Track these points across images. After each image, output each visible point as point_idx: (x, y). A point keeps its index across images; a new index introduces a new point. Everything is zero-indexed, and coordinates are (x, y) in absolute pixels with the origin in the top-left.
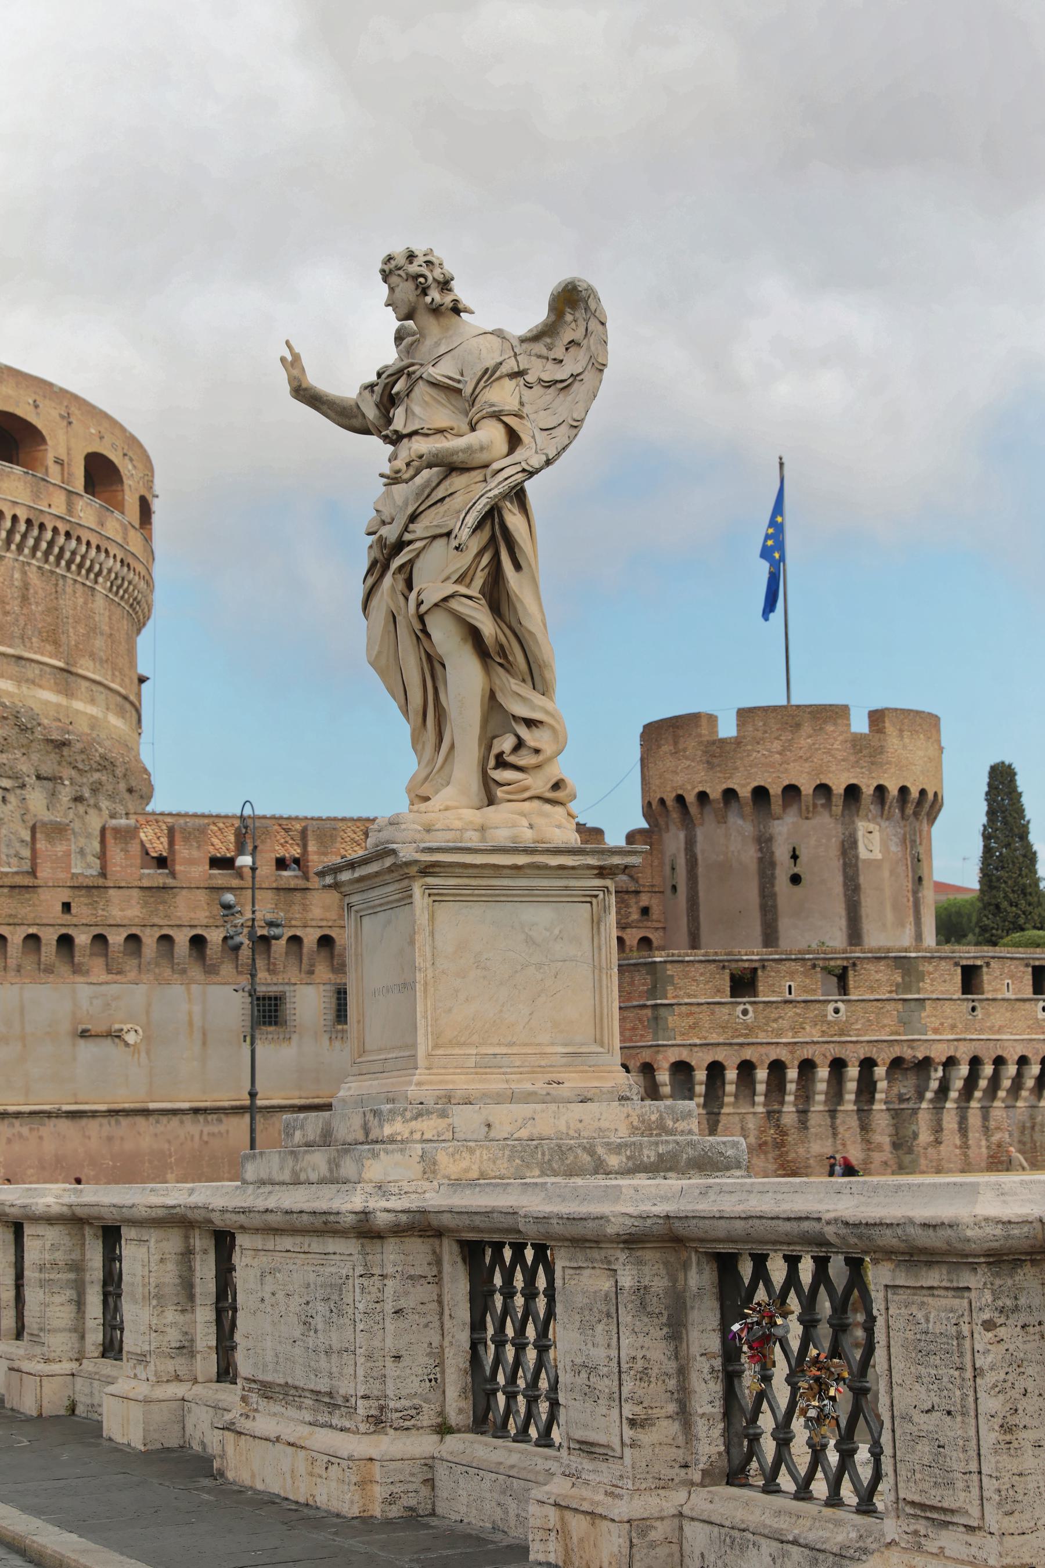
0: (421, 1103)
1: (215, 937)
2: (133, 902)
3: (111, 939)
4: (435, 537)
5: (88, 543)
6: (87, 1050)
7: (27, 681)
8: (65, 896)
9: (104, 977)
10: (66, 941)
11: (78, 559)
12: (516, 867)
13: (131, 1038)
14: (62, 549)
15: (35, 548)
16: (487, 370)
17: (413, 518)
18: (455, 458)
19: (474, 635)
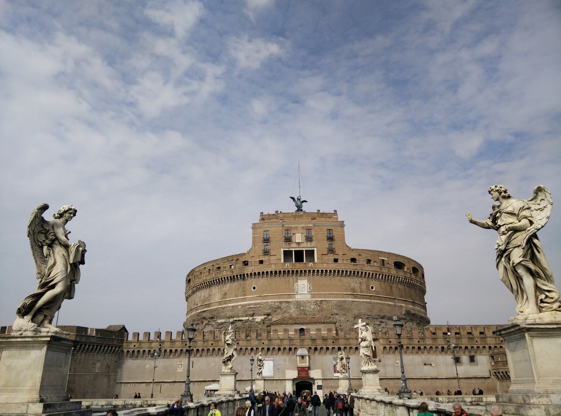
0: (539, 393)
1: (446, 347)
2: (430, 341)
3: (427, 347)
4: (515, 247)
5: (414, 281)
6: (426, 367)
7: (407, 304)
8: (418, 340)
9: (427, 354)
10: (419, 348)
11: (413, 284)
12: (553, 328)
13: (433, 365)
14: (410, 282)
15: (406, 282)
16: (521, 208)
17: (508, 243)
18: (517, 228)
19: (529, 270)
